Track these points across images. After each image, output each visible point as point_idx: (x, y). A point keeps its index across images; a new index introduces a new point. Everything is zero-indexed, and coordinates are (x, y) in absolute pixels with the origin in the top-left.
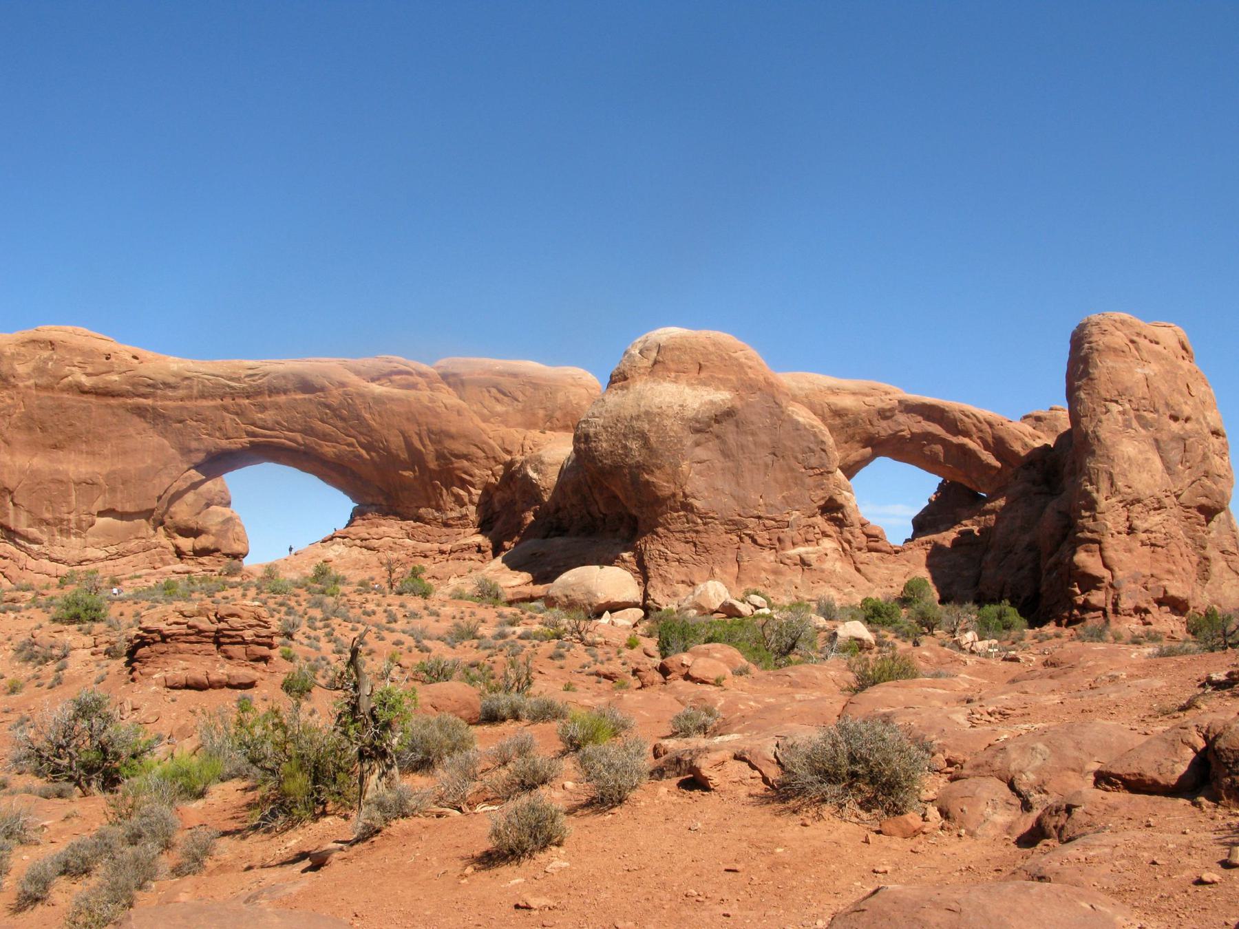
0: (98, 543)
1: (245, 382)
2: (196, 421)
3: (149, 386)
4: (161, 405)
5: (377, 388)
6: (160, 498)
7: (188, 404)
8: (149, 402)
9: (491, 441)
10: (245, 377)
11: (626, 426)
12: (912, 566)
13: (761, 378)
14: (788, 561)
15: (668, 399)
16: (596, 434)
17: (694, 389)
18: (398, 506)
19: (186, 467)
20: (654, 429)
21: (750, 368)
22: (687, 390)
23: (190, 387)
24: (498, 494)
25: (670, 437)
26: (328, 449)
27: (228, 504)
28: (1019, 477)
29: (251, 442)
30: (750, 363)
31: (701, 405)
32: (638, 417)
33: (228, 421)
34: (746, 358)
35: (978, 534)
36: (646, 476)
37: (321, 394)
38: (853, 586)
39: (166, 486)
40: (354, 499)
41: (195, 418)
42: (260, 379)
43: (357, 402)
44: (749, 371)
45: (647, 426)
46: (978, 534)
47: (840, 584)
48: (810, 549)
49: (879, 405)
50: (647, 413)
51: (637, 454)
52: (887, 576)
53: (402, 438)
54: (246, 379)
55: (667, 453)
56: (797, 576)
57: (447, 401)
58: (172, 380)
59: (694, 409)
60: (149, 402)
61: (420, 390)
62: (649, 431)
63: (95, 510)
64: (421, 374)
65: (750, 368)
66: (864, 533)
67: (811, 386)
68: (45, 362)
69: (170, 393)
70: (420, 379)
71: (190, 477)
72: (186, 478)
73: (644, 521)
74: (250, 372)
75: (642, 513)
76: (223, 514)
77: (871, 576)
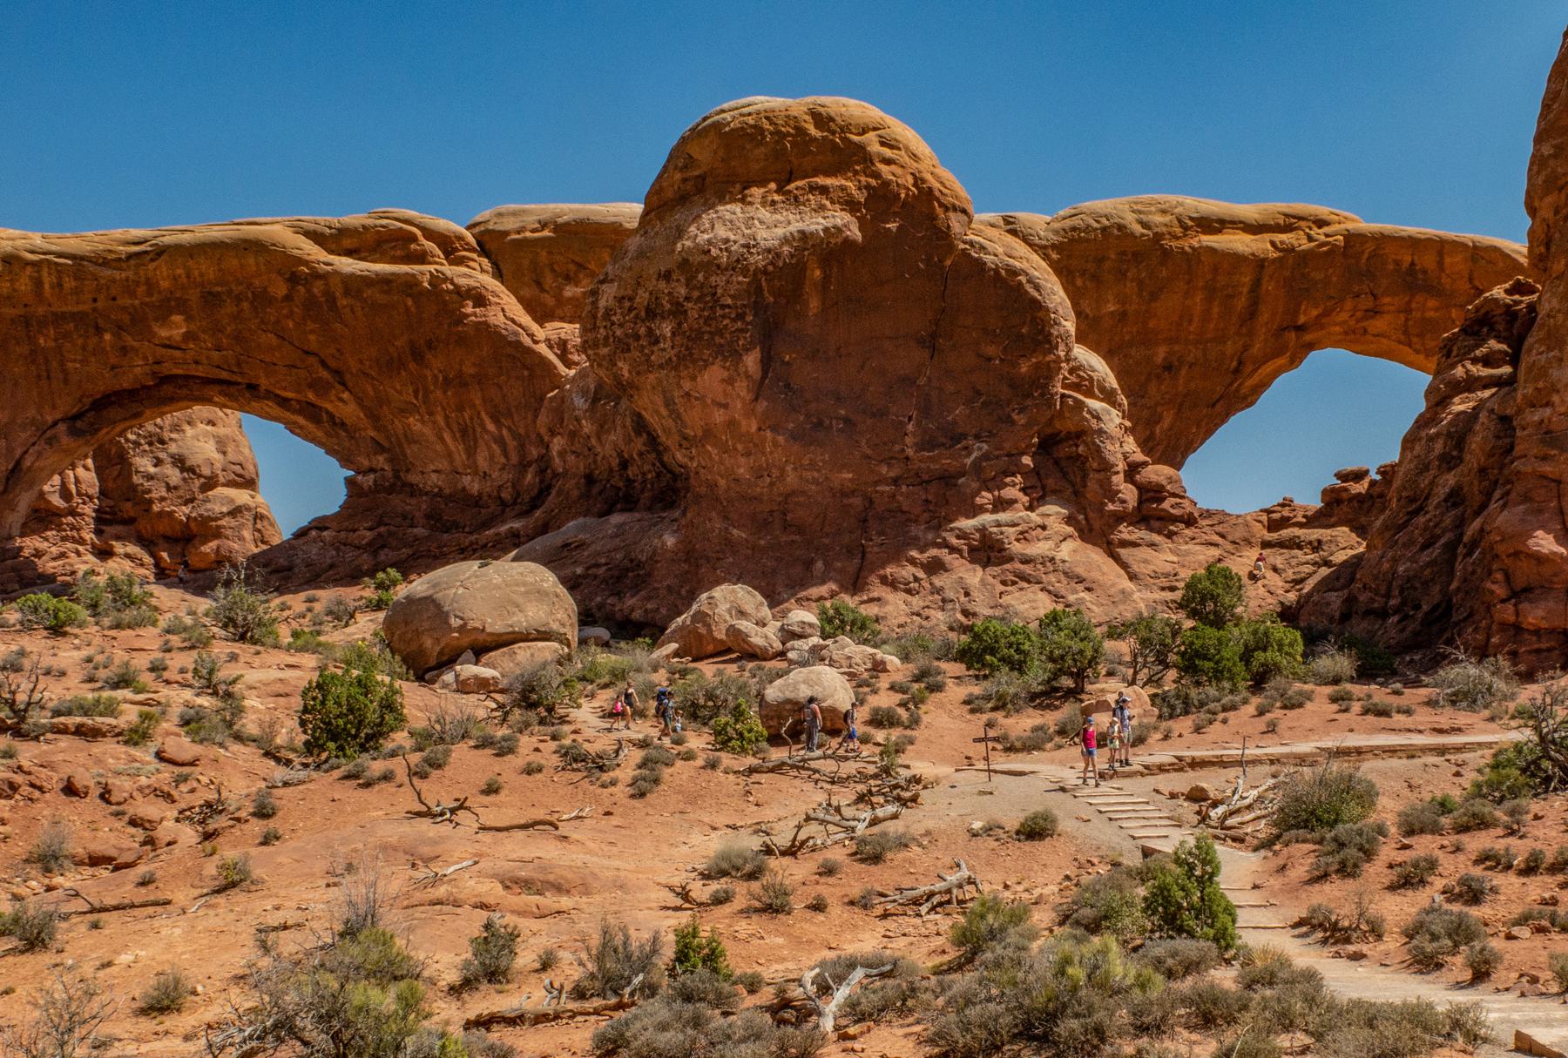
5: (348, 265)
9: (543, 349)
11: (651, 294)
12: (1230, 547)
13: (910, 180)
14: (954, 541)
15: (722, 232)
16: (608, 313)
17: (775, 211)
18: (408, 470)
20: (696, 294)
21: (888, 162)
22: (764, 213)
24: (555, 440)
25: (723, 307)
27: (249, 483)
28: (1454, 353)
30: (887, 152)
31: (786, 240)
32: (667, 276)
34: (883, 144)
35: (1378, 477)
36: (687, 385)
38: (1088, 589)
40: (346, 461)
44: (883, 168)
45: (683, 291)
46: (1378, 477)
47: (1061, 588)
48: (1003, 516)
49: (1306, 245)
50: (684, 264)
51: (668, 344)
52: (1168, 568)
55: (718, 340)
56: (974, 576)
57: (462, 281)
59: (769, 251)
61: (430, 263)
62: (687, 299)
64: (430, 234)
65: (888, 162)
66: (1133, 483)
67: (1167, 219)
70: (430, 246)
73: (697, 473)
75: (691, 459)
76: (232, 501)
77: (1135, 568)
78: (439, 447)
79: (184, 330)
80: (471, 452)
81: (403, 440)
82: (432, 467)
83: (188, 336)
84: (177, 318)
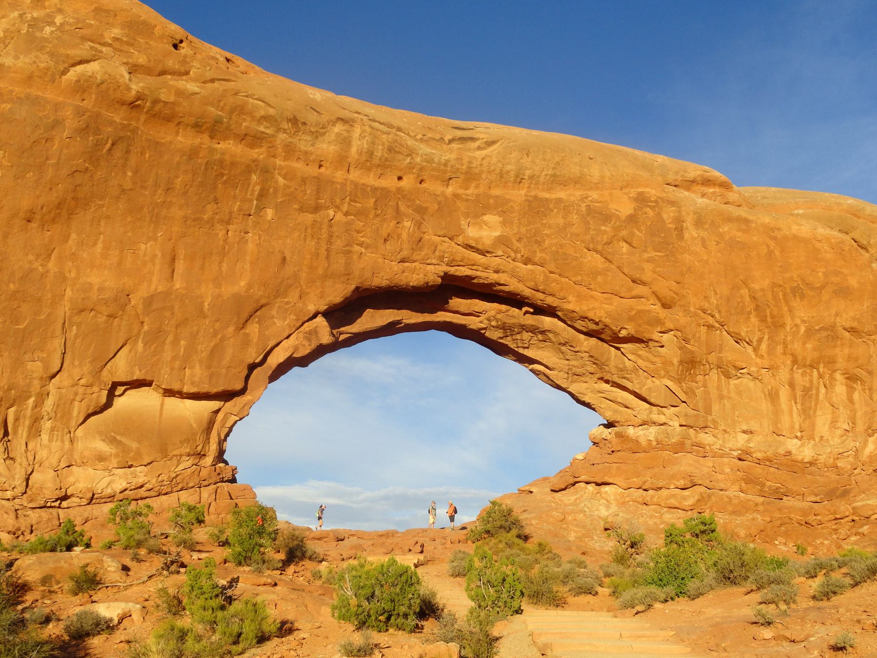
0: (101, 458)
1: (451, 152)
2: (346, 214)
3: (265, 118)
4: (281, 168)
6: (252, 367)
7: (339, 175)
8: (258, 153)
10: (451, 141)
19: (312, 308)
23: (345, 141)
26: (596, 305)
29: (446, 277)
33: (407, 224)
37: (594, 195)
39: (272, 343)
41: (345, 208)
42: (479, 148)
43: (665, 216)
53: (744, 292)
54: (454, 145)
58: (312, 117)
60: (258, 153)
63: (108, 377)
68: (34, 24)
69: (303, 143)
71: (315, 332)
72: (310, 333)
74: (460, 133)
78: (765, 406)
79: (497, 233)
80: (807, 413)
81: (714, 393)
82: (745, 428)
83: (502, 241)
84: (491, 218)
